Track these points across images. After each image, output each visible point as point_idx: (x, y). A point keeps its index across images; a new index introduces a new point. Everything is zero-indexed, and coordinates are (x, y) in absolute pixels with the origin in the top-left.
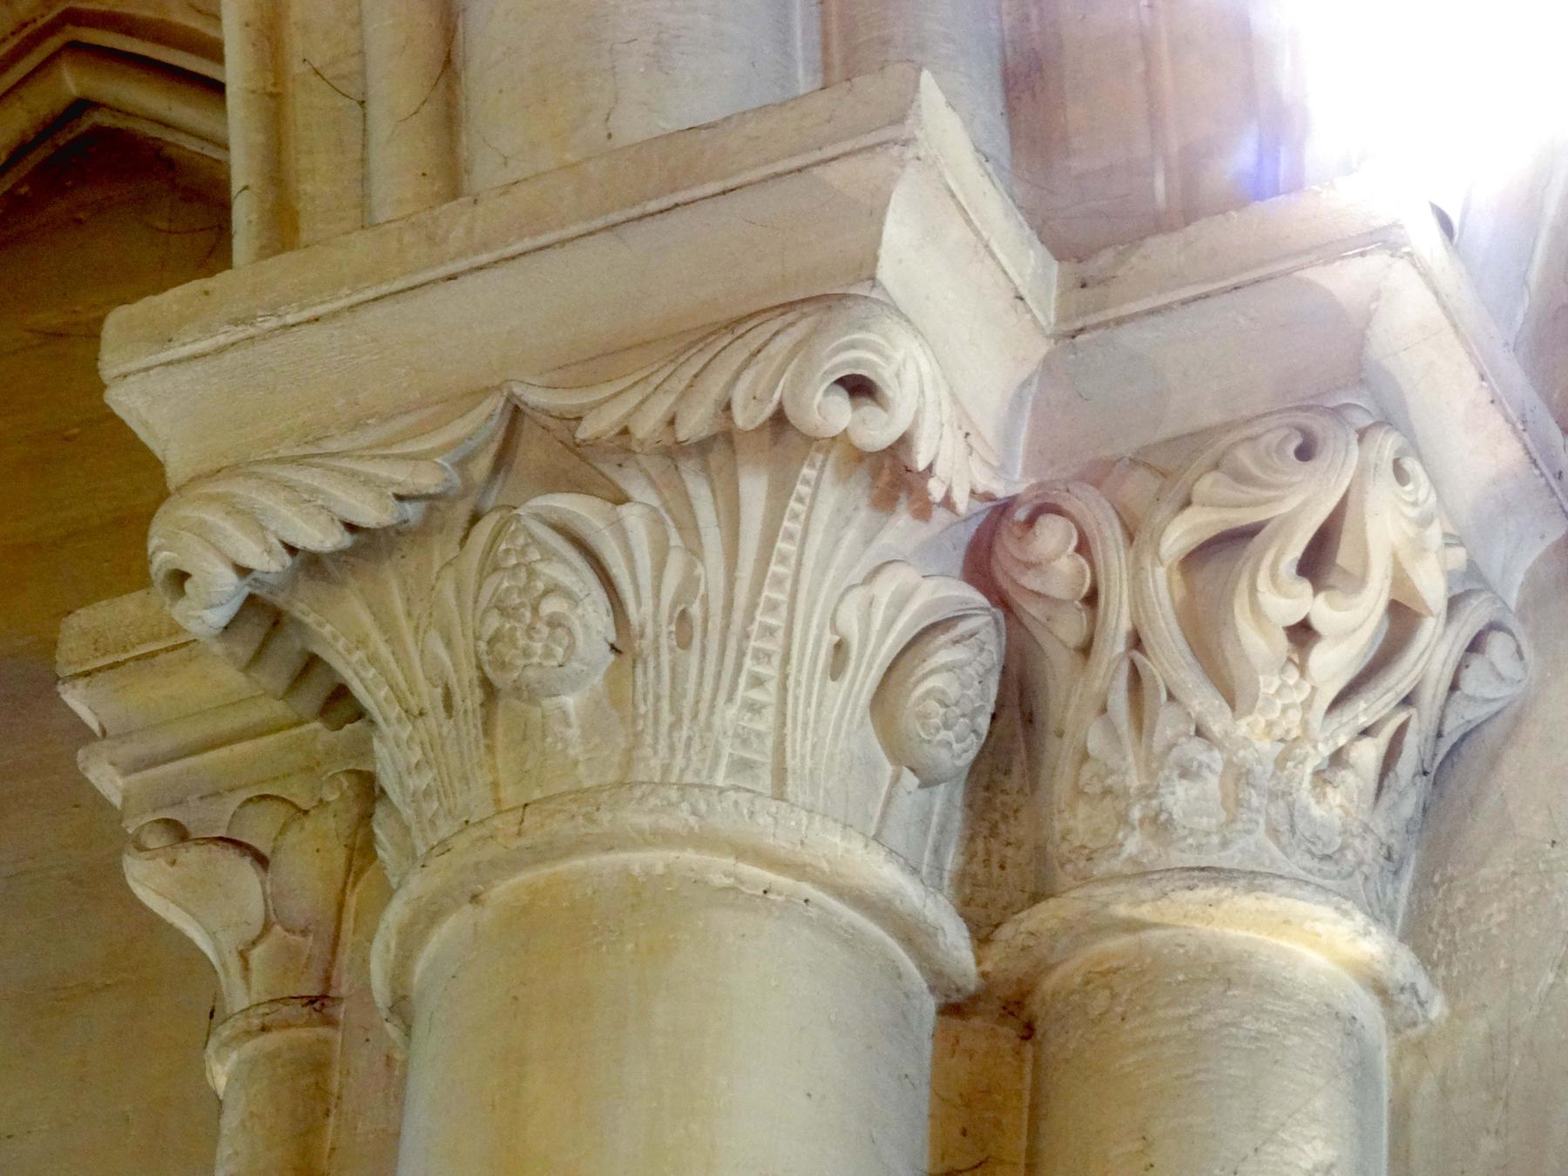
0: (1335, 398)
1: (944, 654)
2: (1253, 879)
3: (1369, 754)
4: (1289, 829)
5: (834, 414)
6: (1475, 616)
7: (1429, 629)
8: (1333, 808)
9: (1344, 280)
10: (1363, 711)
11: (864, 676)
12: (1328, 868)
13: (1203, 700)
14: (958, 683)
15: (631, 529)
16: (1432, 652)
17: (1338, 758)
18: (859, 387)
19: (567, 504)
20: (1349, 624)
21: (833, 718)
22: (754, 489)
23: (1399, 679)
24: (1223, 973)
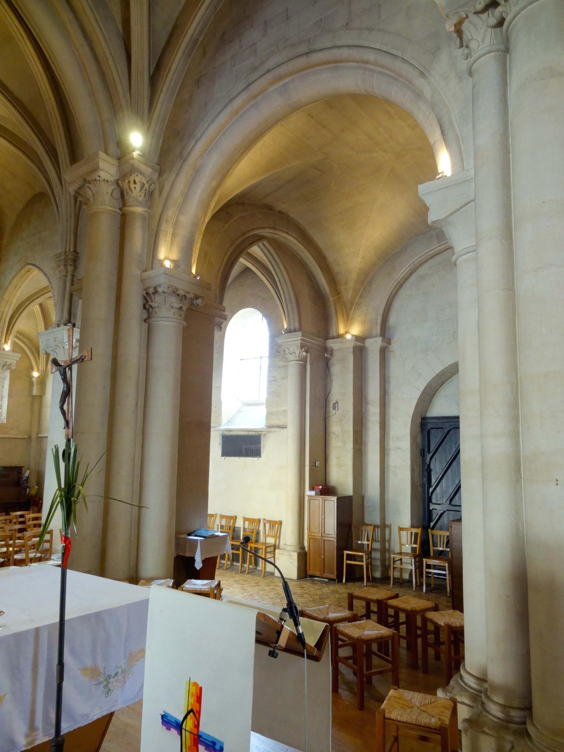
0: (133, 170)
1: (114, 191)
2: (133, 206)
3: (143, 195)
4: (137, 201)
5: (98, 178)
6: (149, 183)
7: (146, 185)
8: (141, 199)
9: (132, 161)
10: (142, 192)
11: (109, 194)
12: (140, 204)
13: (130, 193)
14: (117, 194)
15: (92, 186)
16: (146, 186)
17: (141, 195)
18: (99, 176)
19: (89, 185)
20: (138, 186)
21: (107, 198)
22: (98, 183)
23: (144, 188)
24: (132, 213)
